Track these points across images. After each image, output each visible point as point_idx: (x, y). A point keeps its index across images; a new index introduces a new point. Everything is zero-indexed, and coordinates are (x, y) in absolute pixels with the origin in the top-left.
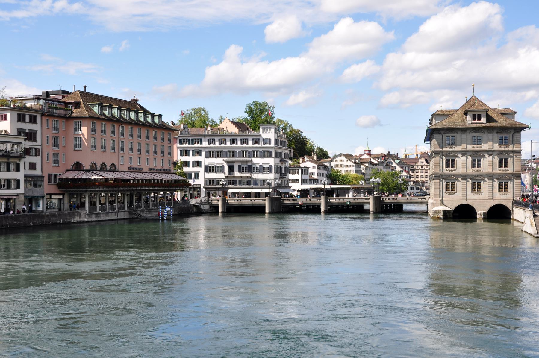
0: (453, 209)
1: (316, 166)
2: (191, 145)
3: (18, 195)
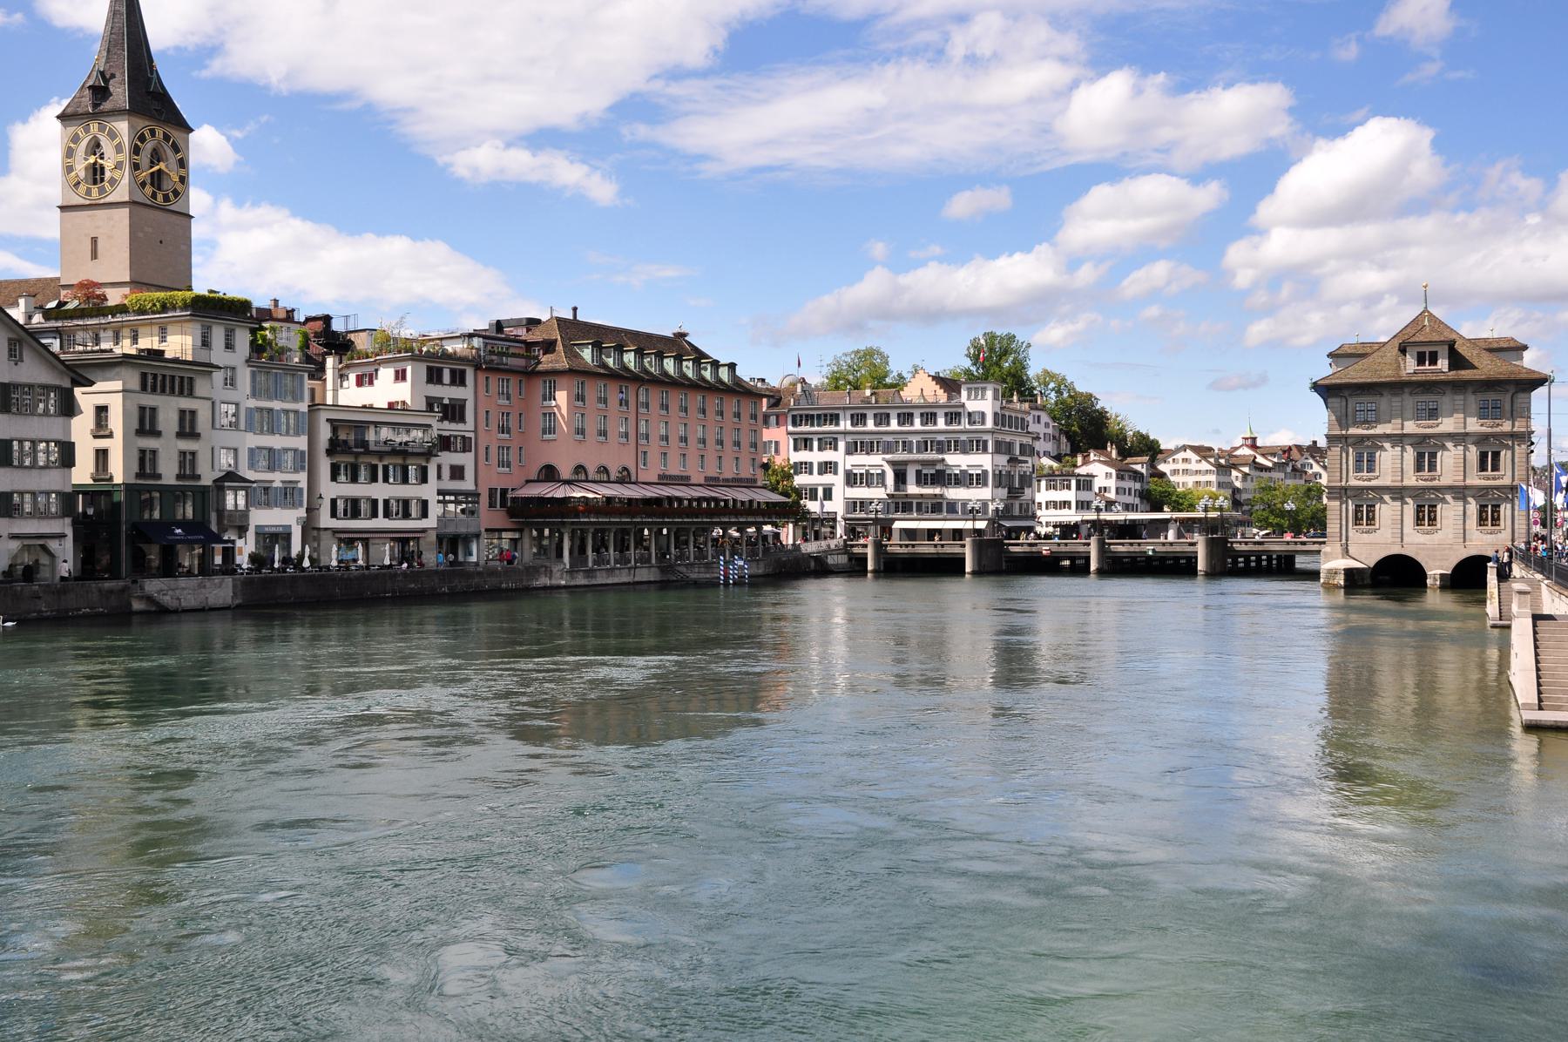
0: (1372, 566)
1: (1113, 472)
2: (816, 429)
3: (424, 531)
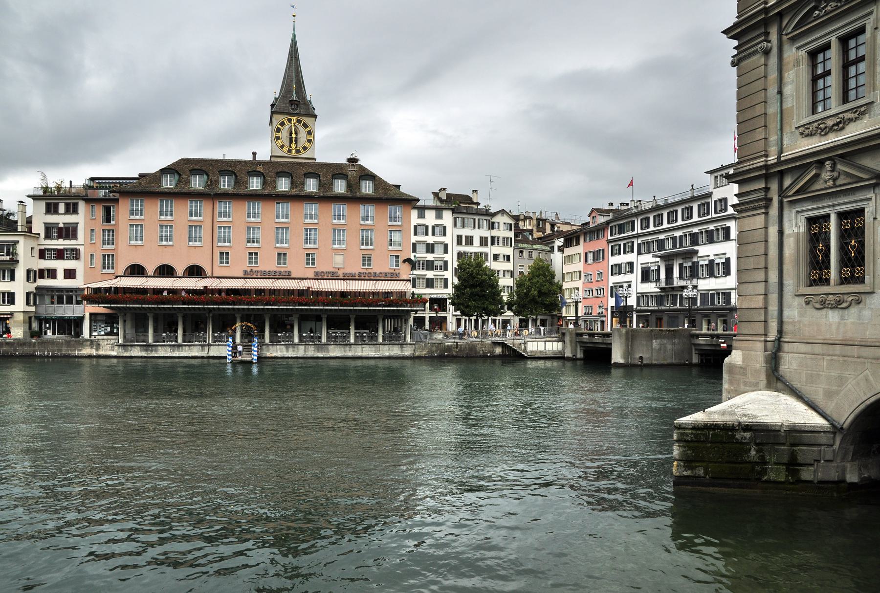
0: (845, 415)
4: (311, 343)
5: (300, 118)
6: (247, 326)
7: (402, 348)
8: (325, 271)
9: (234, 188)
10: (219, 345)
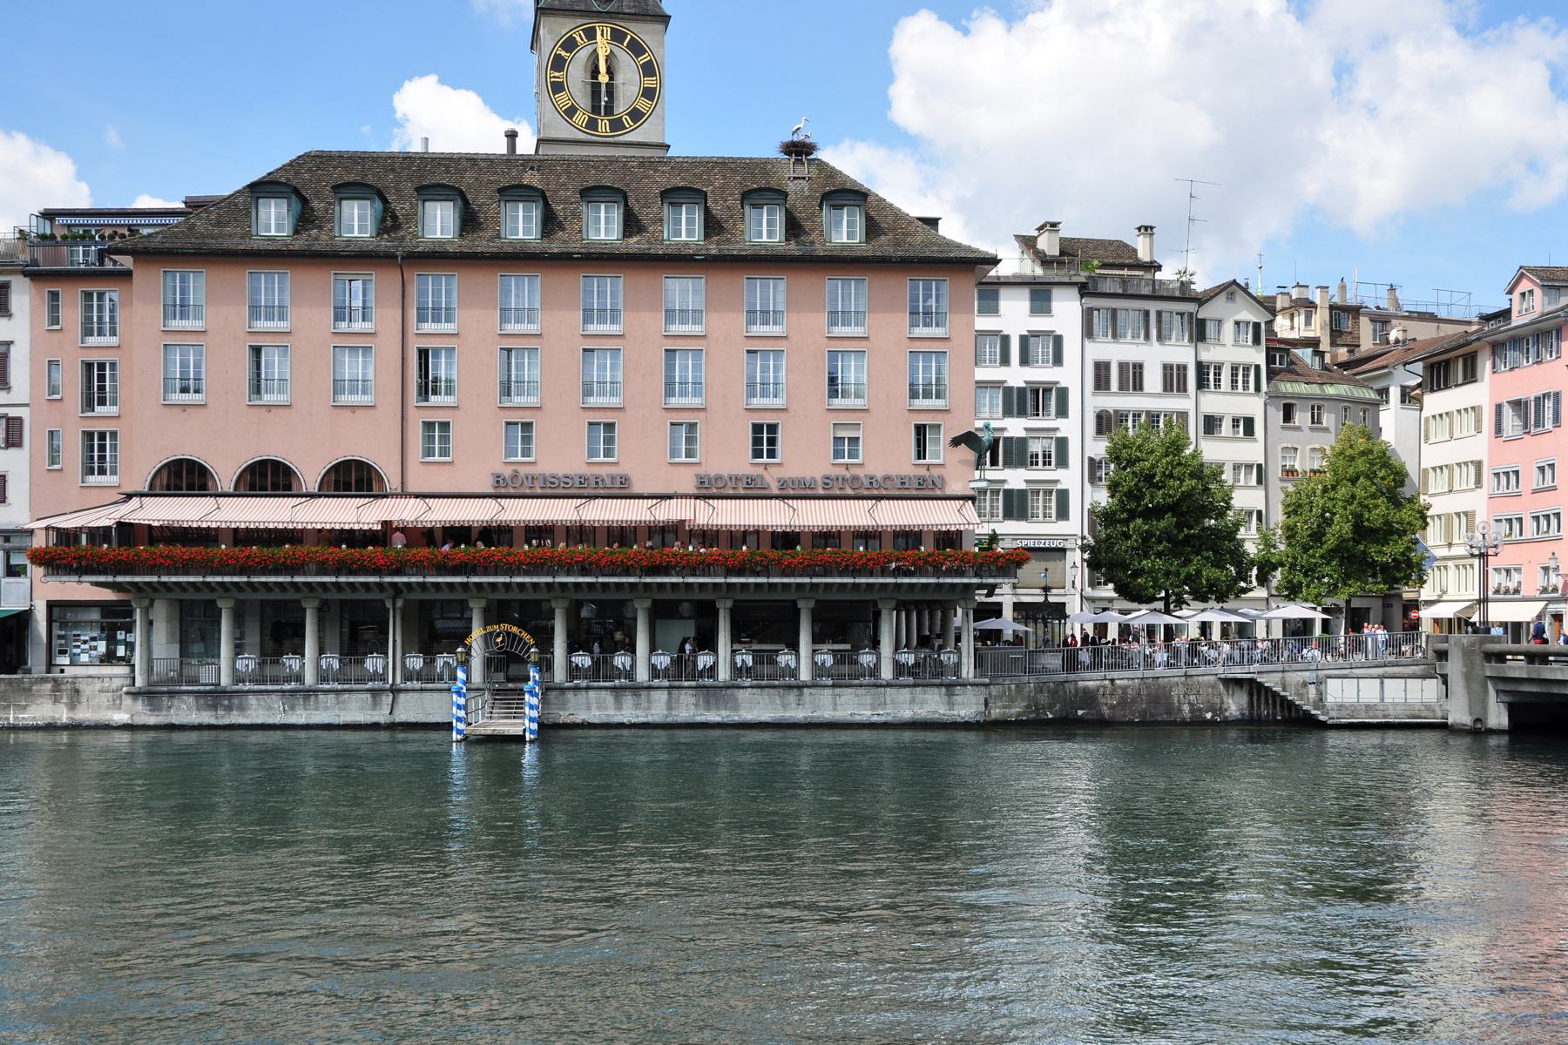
4: (686, 684)
5: (621, 25)
6: (509, 634)
7: (950, 694)
8: (725, 475)
9: (461, 236)
10: (422, 690)
